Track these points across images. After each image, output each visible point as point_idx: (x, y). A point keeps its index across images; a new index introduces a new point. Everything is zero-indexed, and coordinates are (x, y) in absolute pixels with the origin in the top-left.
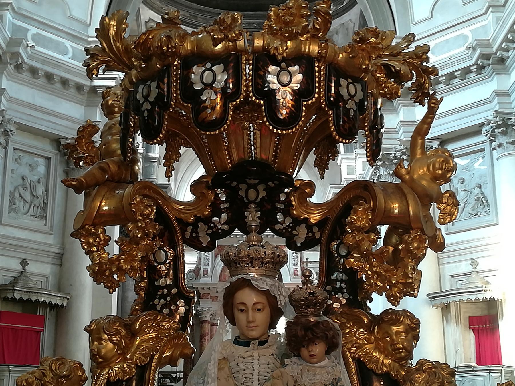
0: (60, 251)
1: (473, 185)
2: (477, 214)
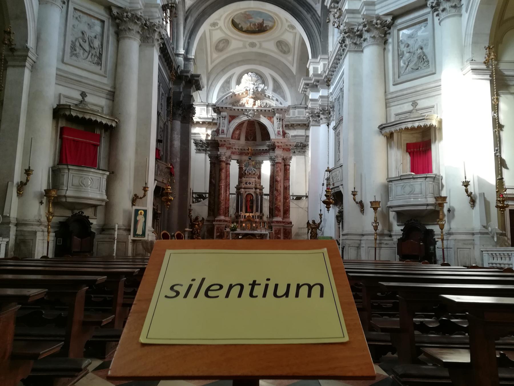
0: (112, 90)
1: (417, 46)
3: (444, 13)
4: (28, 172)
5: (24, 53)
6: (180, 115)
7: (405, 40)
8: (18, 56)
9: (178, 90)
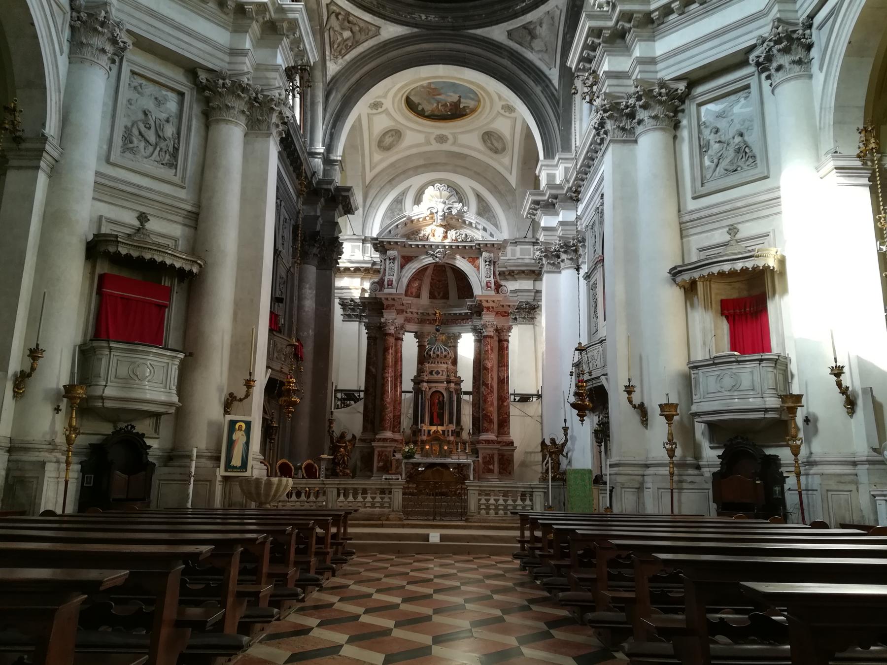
0: (194, 210)
1: (732, 131)
2: (736, 170)
3: (780, 73)
4: (34, 354)
5: (38, 146)
6: (315, 255)
7: (712, 120)
8: (27, 150)
9: (312, 214)
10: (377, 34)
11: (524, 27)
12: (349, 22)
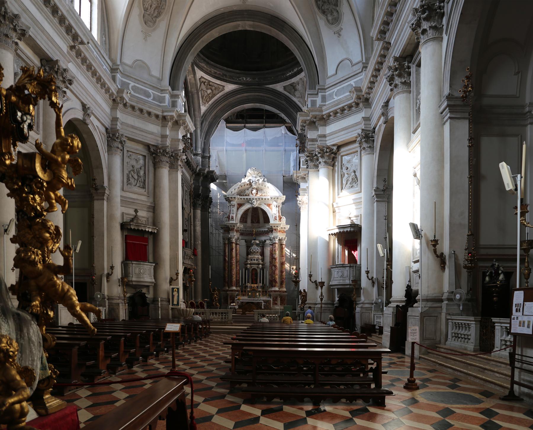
10: (223, 90)
11: (292, 85)
12: (210, 85)
